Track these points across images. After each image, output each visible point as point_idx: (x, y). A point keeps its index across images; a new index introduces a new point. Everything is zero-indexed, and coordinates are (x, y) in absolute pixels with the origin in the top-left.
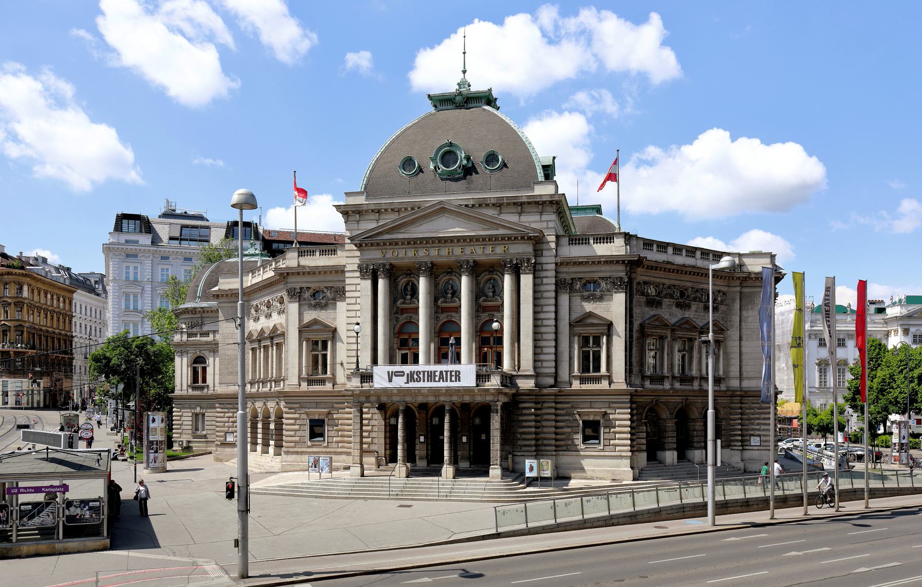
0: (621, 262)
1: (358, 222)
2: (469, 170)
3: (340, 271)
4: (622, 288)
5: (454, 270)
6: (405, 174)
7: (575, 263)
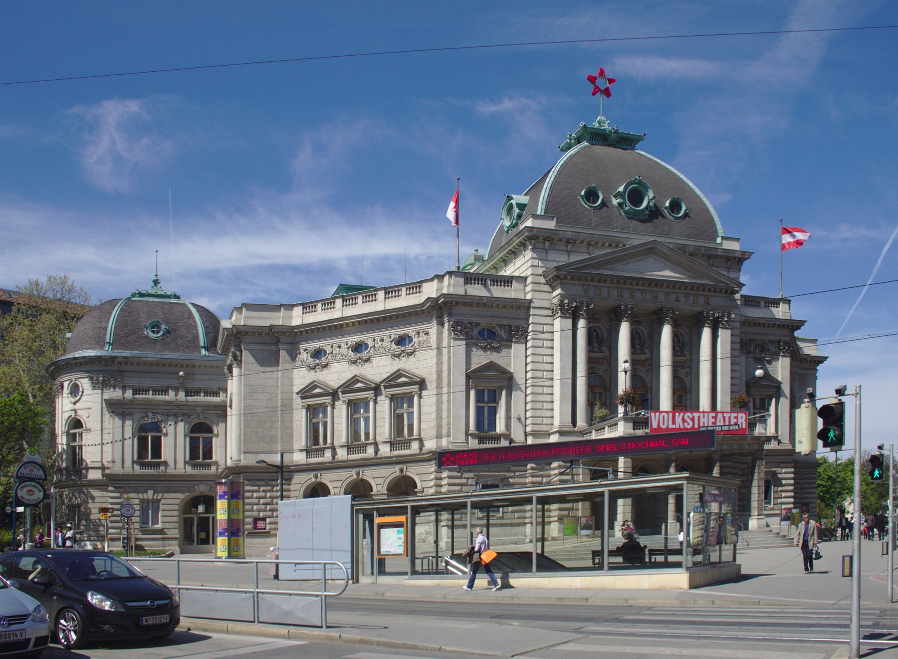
0: (790, 327)
1: (546, 251)
2: (654, 213)
3: (524, 306)
4: (788, 353)
5: (657, 319)
6: (588, 205)
7: (754, 324)
